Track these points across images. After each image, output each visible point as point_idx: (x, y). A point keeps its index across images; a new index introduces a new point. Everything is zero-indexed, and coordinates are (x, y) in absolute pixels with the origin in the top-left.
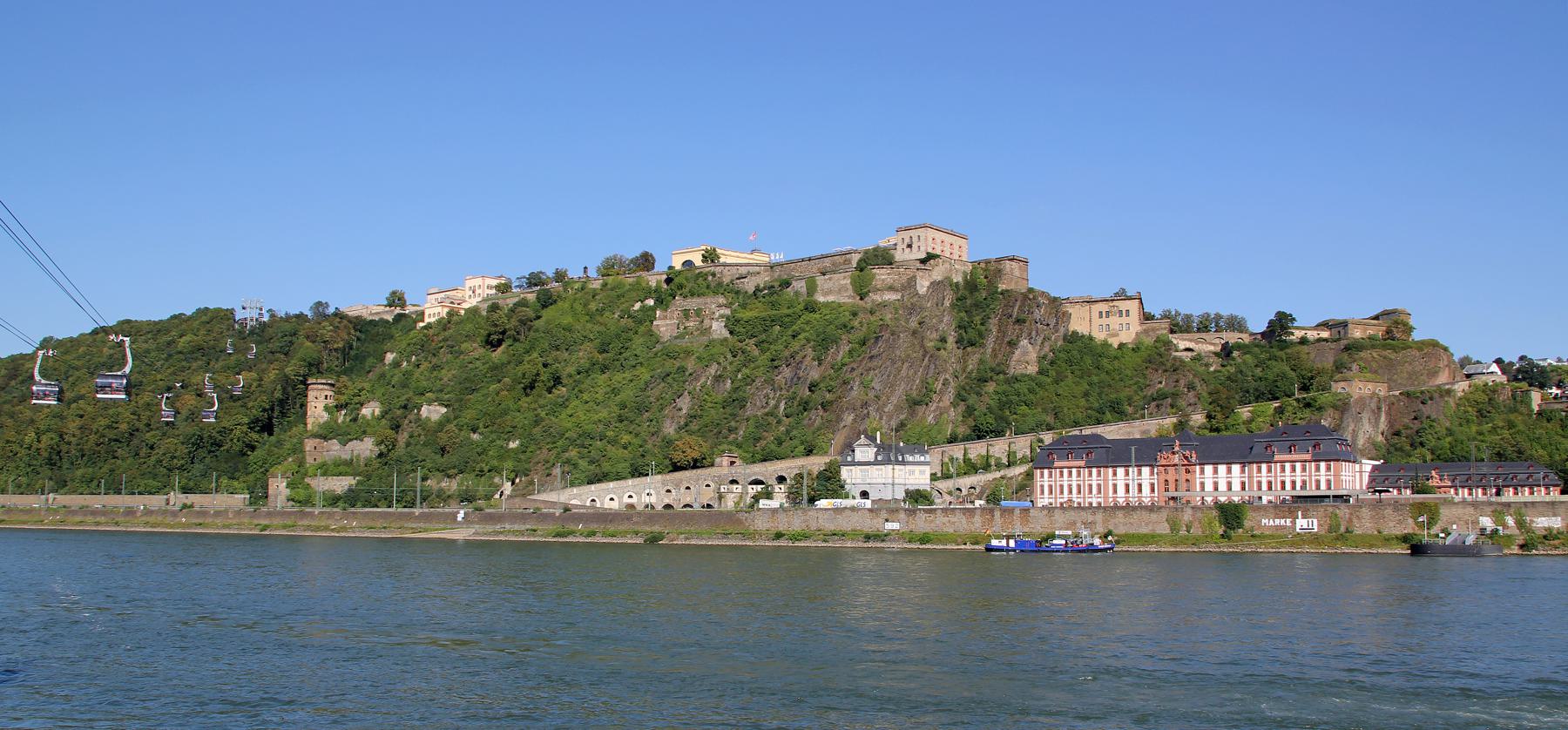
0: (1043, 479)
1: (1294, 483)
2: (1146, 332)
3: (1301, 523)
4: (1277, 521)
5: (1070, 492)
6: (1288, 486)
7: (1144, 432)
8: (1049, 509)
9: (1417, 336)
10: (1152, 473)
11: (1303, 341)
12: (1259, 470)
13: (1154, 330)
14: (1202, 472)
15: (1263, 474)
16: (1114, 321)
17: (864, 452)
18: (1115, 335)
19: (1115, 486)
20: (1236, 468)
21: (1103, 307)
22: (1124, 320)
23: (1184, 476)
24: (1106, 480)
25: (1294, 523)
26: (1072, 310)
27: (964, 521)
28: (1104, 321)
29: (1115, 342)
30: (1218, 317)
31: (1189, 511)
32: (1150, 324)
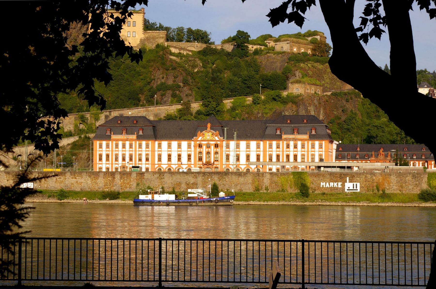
0: (101, 148)
1: (295, 157)
2: (147, 39)
3: (349, 185)
4: (332, 184)
5: (124, 159)
6: (292, 159)
7: (156, 115)
8: (108, 173)
10: (189, 146)
11: (256, 52)
13: (154, 38)
14: (228, 146)
15: (273, 148)
19: (160, 156)
23: (212, 150)
24: (153, 151)
25: (343, 185)
27: (89, 182)
30: (190, 30)
31: (268, 176)
32: (151, 33)
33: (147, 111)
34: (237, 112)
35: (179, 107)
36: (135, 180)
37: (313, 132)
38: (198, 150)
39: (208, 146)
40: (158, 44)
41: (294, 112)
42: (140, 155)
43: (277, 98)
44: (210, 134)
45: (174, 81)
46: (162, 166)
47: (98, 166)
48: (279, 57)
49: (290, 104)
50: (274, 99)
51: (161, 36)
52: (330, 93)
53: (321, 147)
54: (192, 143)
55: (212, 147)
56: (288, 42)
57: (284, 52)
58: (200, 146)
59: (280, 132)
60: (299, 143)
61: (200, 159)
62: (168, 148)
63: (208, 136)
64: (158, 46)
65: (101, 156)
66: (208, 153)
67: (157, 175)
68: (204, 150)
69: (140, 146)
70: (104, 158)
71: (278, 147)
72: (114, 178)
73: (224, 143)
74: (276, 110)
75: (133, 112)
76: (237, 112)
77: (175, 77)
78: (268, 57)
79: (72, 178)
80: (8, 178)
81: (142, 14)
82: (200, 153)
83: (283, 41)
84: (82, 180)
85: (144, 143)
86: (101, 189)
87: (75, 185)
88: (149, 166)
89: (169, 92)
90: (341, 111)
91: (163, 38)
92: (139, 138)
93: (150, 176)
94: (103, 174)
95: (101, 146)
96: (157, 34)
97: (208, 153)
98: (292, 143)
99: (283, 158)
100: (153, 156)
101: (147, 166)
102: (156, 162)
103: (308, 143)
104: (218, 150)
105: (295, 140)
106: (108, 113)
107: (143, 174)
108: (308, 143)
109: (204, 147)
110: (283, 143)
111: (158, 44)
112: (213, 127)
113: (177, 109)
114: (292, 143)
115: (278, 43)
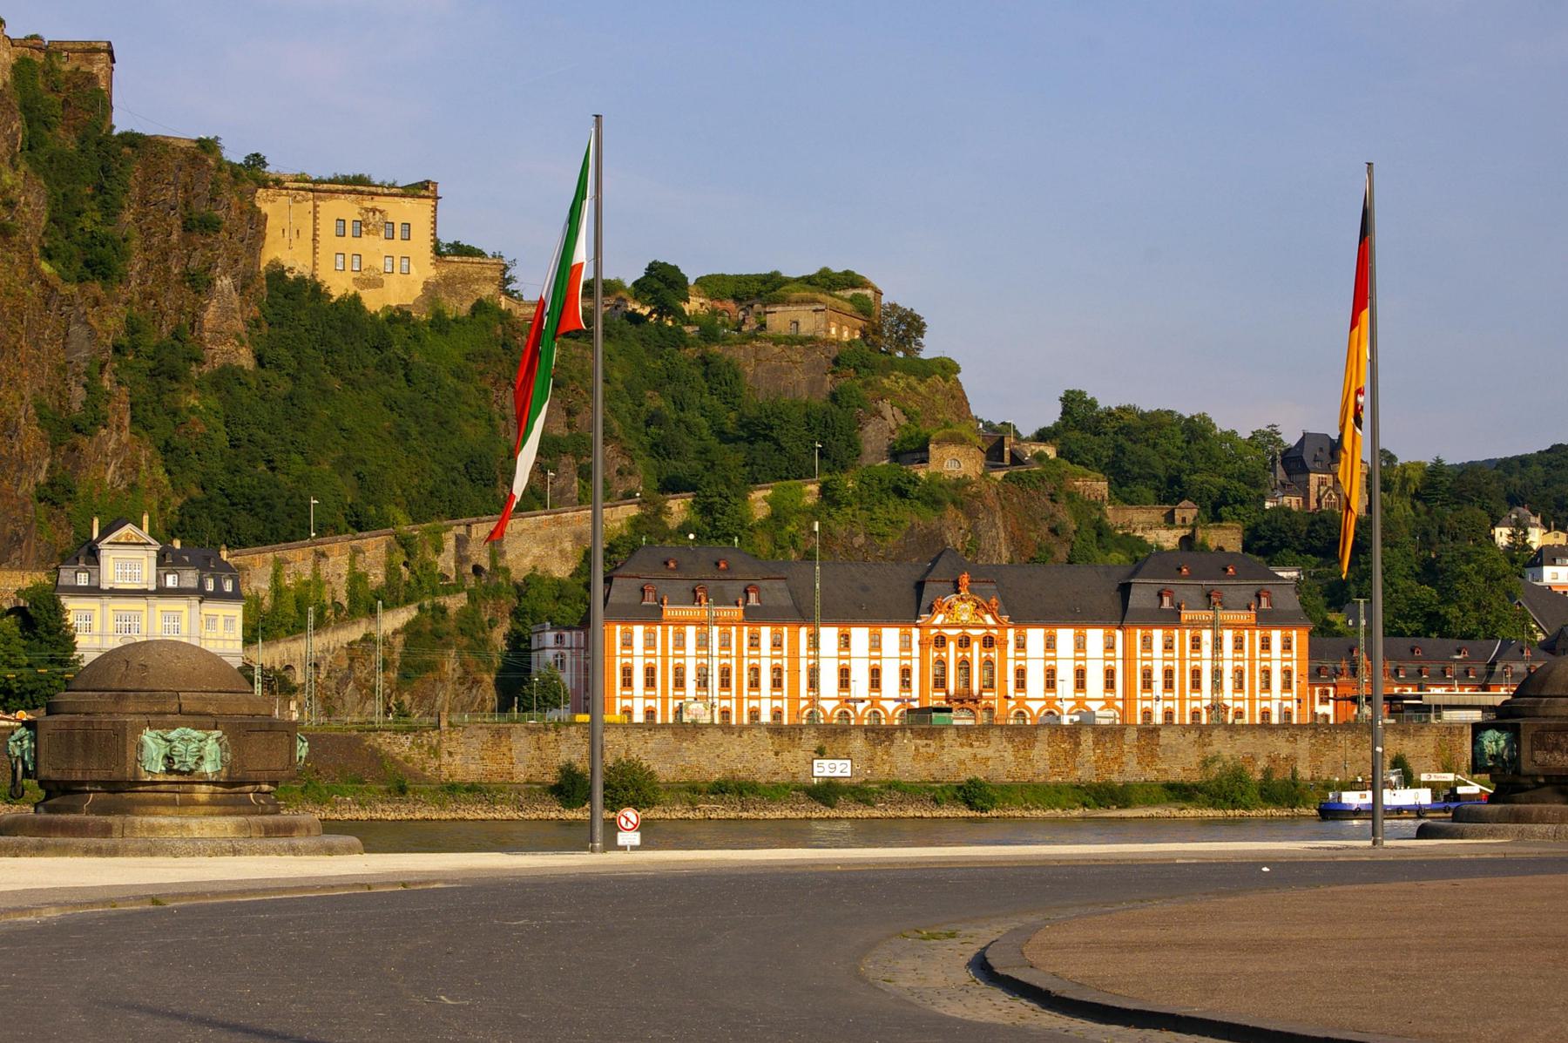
0: (631, 648)
2: (448, 283)
9: (931, 347)
10: (906, 645)
12: (1147, 644)
13: (466, 280)
14: (1021, 645)
15: (1157, 650)
16: (374, 249)
17: (128, 561)
18: (375, 283)
19: (814, 673)
20: (1095, 637)
21: (346, 208)
22: (397, 246)
23: (976, 653)
24: (794, 657)
26: (270, 205)
27: (1009, 756)
28: (350, 244)
29: (373, 302)
32: (457, 264)
33: (558, 523)
34: (789, 528)
35: (633, 510)
36: (1135, 750)
37: (1264, 605)
38: (933, 654)
39: (965, 642)
40: (480, 301)
41: (965, 535)
42: (755, 670)
43: (910, 487)
44: (969, 606)
45: (569, 426)
46: (882, 703)
47: (619, 704)
48: (796, 354)
49: (950, 511)
50: (901, 493)
51: (489, 273)
52: (1003, 473)
53: (1287, 646)
54: (916, 632)
55: (976, 646)
56: (819, 307)
57: (811, 339)
58: (941, 642)
59: (1172, 603)
60: (1228, 636)
61: (940, 683)
62: (872, 648)
63: (960, 613)
64: (480, 307)
65: (627, 672)
66: (965, 666)
67: (1193, 735)
68: (952, 653)
69: (755, 643)
70: (639, 678)
71: (1168, 647)
72: (1078, 744)
73: (1011, 633)
74: (912, 528)
75: (525, 526)
76: (789, 528)
77: (570, 413)
78: (757, 350)
79: (962, 745)
80: (777, 748)
81: (430, 202)
82: (942, 663)
83: (797, 303)
84: (990, 752)
85: (766, 632)
86: (1042, 778)
87: (970, 764)
88: (784, 705)
89: (567, 460)
90: (1046, 530)
91: (493, 280)
92: (754, 617)
93: (1173, 736)
94: (1047, 731)
95: (628, 644)
96: (477, 268)
97: (965, 666)
98: (1207, 635)
99: (1182, 680)
100: (795, 671)
101: (777, 703)
102: (803, 692)
103: (1252, 636)
104: (994, 654)
105: (1214, 626)
106: (462, 530)
107: (1156, 730)
108: (1252, 636)
109: (952, 645)
110: (1182, 636)
111: (480, 301)
112: (976, 586)
113: (629, 518)
114: (1207, 635)
115: (779, 309)
